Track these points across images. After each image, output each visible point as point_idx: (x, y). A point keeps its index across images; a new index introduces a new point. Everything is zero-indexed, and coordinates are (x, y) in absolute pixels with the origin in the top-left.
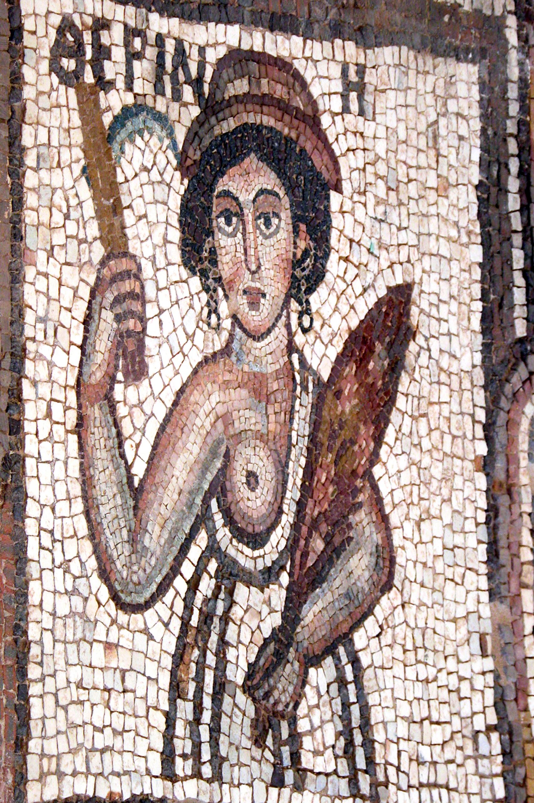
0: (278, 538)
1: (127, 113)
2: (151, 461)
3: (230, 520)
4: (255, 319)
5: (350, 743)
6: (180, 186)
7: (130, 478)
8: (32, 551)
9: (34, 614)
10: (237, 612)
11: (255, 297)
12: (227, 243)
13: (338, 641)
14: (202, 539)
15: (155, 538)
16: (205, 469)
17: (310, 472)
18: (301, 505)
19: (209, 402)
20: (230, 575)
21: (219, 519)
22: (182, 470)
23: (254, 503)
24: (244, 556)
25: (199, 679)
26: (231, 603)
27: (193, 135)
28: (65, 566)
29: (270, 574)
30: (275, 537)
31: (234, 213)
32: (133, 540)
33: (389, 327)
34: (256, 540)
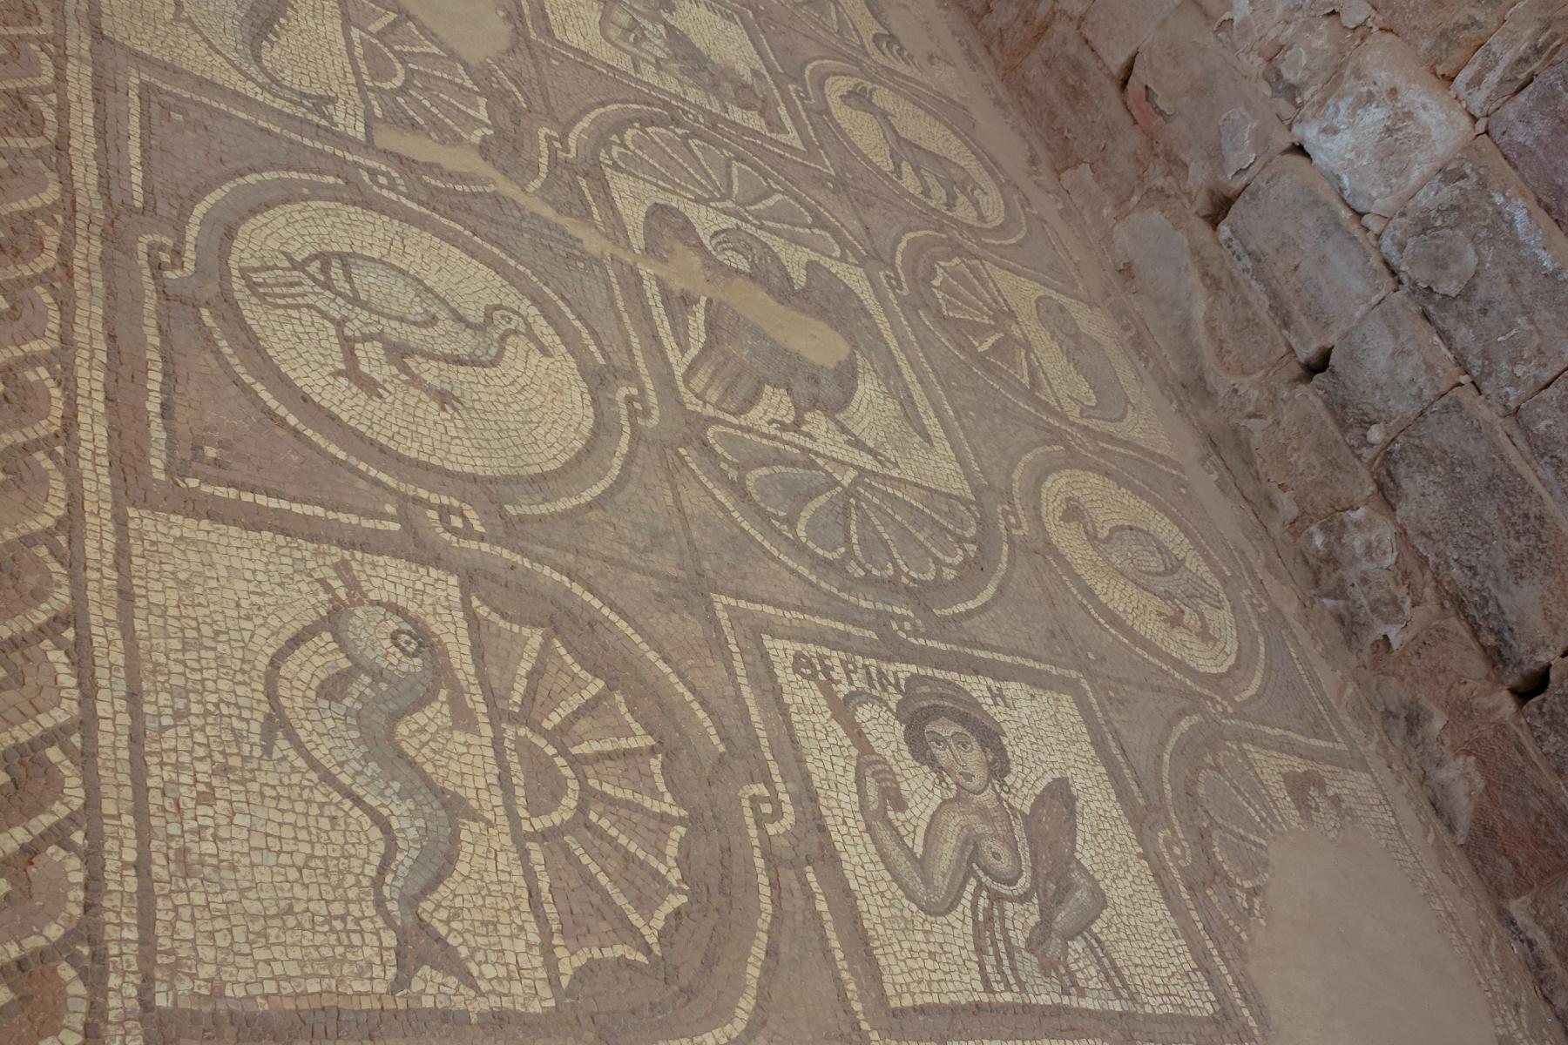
0: (1024, 882)
1: (851, 695)
2: (925, 846)
3: (987, 873)
4: (976, 783)
5: (1108, 978)
6: (900, 729)
7: (914, 855)
8: (853, 885)
9: (865, 916)
10: (1009, 914)
11: (969, 777)
12: (943, 755)
13: (1081, 928)
14: (973, 882)
15: (938, 881)
16: (962, 851)
17: (1034, 855)
18: (1033, 869)
19: (954, 823)
20: (996, 898)
21: (981, 873)
22: (948, 851)
23: (1004, 865)
24: (1004, 889)
25: (994, 944)
26: (1002, 911)
27: (899, 704)
28: (882, 894)
29: (1024, 898)
30: (1022, 881)
31: (940, 740)
32: (927, 882)
33: (1060, 796)
34: (1012, 882)
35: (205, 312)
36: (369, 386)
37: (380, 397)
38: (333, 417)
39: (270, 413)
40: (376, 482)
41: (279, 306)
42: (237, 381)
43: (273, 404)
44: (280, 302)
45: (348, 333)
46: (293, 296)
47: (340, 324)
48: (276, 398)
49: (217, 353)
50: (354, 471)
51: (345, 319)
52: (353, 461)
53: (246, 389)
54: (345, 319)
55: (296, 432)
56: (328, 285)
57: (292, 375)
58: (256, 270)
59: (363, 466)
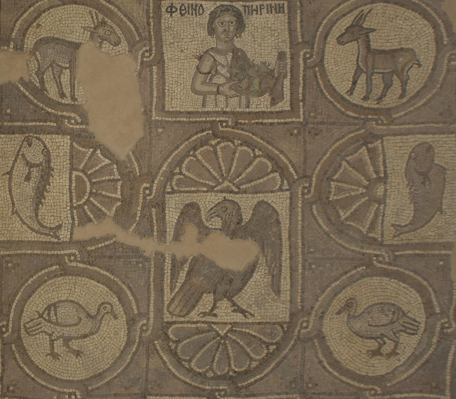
35: (13, 345)
36: (54, 356)
37: (59, 359)
38: (44, 372)
39: (27, 375)
40: (53, 390)
41: (33, 335)
42: (20, 367)
43: (28, 371)
44: (34, 333)
45: (53, 338)
46: (38, 329)
47: (50, 335)
48: (29, 370)
49: (15, 359)
50: (47, 388)
51: (53, 333)
52: (48, 385)
53: (22, 368)
54: (53, 333)
55: (33, 379)
56: (49, 321)
57: (34, 360)
58: (28, 323)
59: (50, 386)
